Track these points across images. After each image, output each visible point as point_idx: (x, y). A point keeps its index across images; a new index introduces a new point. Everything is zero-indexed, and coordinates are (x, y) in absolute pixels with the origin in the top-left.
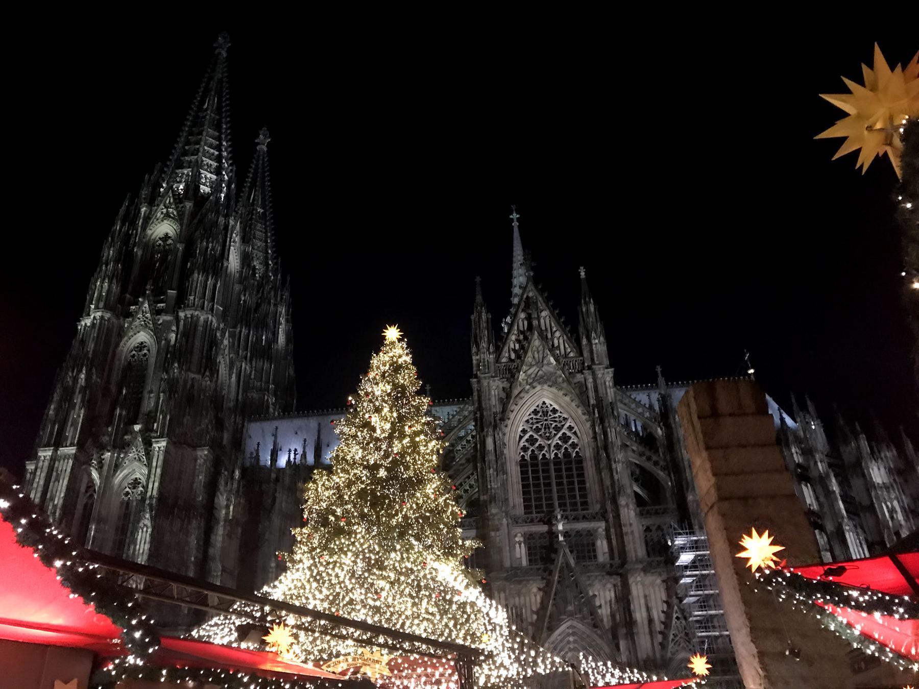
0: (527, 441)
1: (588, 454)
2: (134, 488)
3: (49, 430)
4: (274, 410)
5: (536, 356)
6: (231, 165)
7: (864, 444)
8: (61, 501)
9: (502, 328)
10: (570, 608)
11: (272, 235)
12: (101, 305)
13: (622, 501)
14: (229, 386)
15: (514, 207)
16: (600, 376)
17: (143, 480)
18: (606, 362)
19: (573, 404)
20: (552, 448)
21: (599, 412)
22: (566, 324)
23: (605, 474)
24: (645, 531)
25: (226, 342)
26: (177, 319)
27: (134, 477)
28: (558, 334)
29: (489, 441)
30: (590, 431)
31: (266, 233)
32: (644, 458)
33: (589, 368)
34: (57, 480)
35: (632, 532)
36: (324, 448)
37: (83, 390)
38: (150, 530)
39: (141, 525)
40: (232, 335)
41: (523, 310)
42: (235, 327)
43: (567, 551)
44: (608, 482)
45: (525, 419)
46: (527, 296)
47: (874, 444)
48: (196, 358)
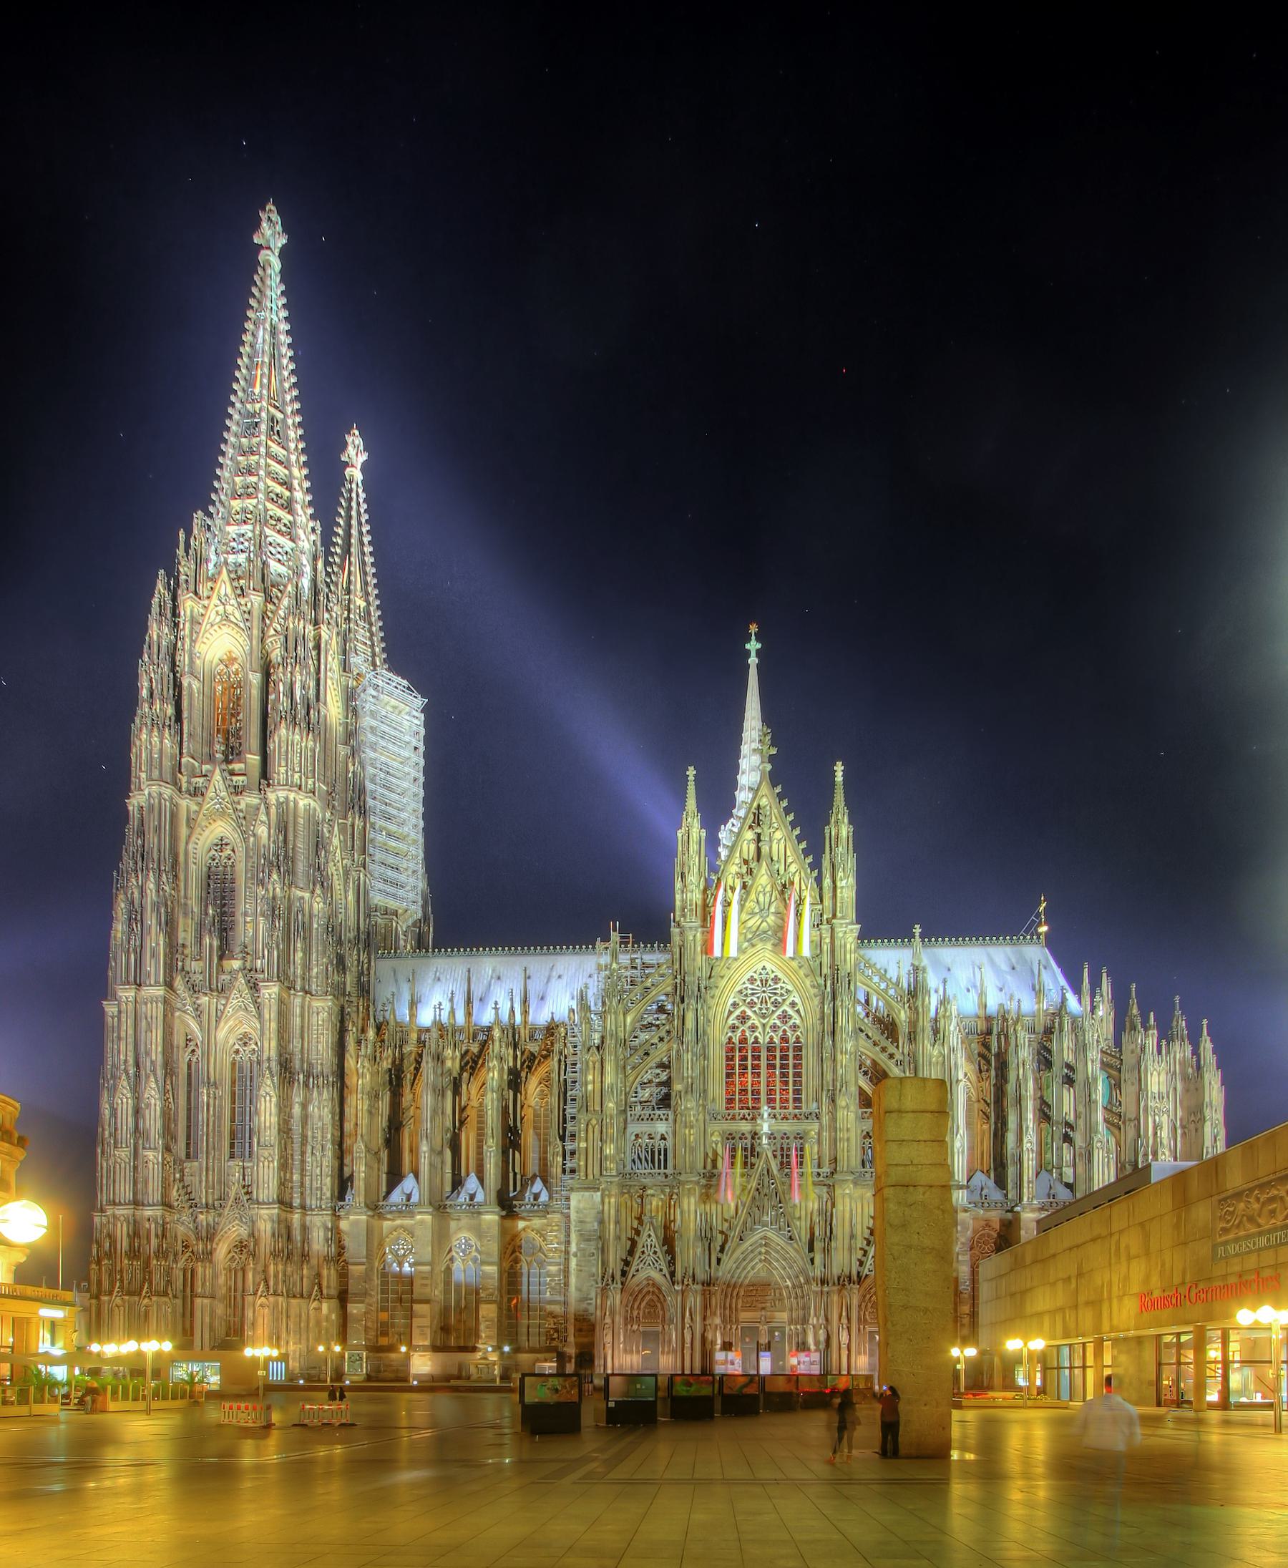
0: (737, 1018)
1: (809, 1041)
2: (245, 1044)
3: (120, 963)
4: (405, 941)
5: (761, 899)
6: (313, 517)
7: (1151, 1041)
8: (160, 1057)
9: (718, 855)
10: (766, 1218)
11: (384, 650)
12: (156, 773)
13: (842, 1101)
14: (346, 908)
15: (753, 629)
16: (841, 935)
17: (255, 1035)
18: (852, 914)
19: (801, 973)
20: (768, 1029)
21: (833, 985)
22: (806, 853)
23: (828, 1065)
24: (865, 1138)
25: (336, 841)
26: (265, 800)
27: (242, 1031)
28: (793, 868)
29: (690, 1017)
30: (818, 1010)
31: (372, 646)
32: (878, 1049)
33: (828, 922)
34: (149, 1029)
35: (848, 1140)
36: (476, 1004)
37: (156, 906)
38: (274, 1099)
39: (262, 1092)
40: (343, 830)
41: (750, 827)
42: (345, 818)
43: (770, 1155)
44: (829, 1077)
45: (738, 989)
46: (759, 807)
47: (1164, 1043)
48: (301, 867)
